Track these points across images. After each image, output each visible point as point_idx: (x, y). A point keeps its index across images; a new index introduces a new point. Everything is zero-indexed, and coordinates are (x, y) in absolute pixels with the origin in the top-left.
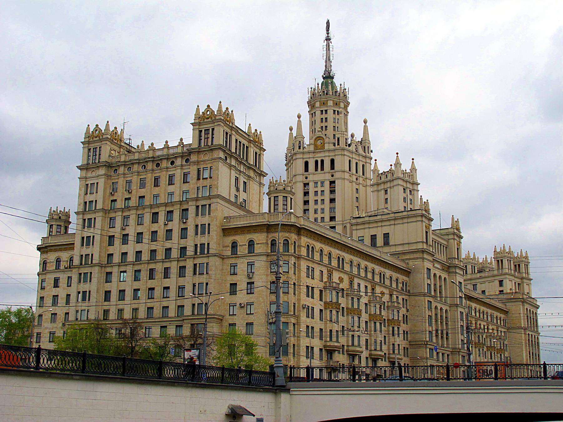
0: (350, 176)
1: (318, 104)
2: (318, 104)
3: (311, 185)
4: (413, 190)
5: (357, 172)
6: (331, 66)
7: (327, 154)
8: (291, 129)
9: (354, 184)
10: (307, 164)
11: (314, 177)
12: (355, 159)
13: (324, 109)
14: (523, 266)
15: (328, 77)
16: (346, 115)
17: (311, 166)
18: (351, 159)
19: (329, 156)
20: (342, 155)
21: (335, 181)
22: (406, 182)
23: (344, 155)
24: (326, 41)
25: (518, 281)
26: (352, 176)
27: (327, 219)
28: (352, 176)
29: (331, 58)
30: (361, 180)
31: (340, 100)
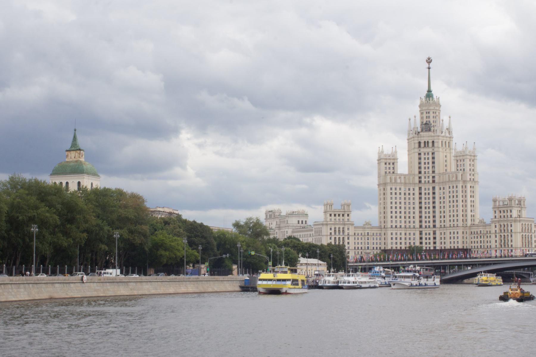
3: (422, 154)
5: (445, 147)
7: (430, 138)
8: (410, 120)
10: (420, 143)
11: (423, 150)
13: (428, 111)
14: (522, 202)
15: (429, 91)
17: (422, 145)
19: (431, 139)
21: (434, 153)
22: (471, 156)
25: (519, 209)
27: (431, 172)
30: (448, 150)
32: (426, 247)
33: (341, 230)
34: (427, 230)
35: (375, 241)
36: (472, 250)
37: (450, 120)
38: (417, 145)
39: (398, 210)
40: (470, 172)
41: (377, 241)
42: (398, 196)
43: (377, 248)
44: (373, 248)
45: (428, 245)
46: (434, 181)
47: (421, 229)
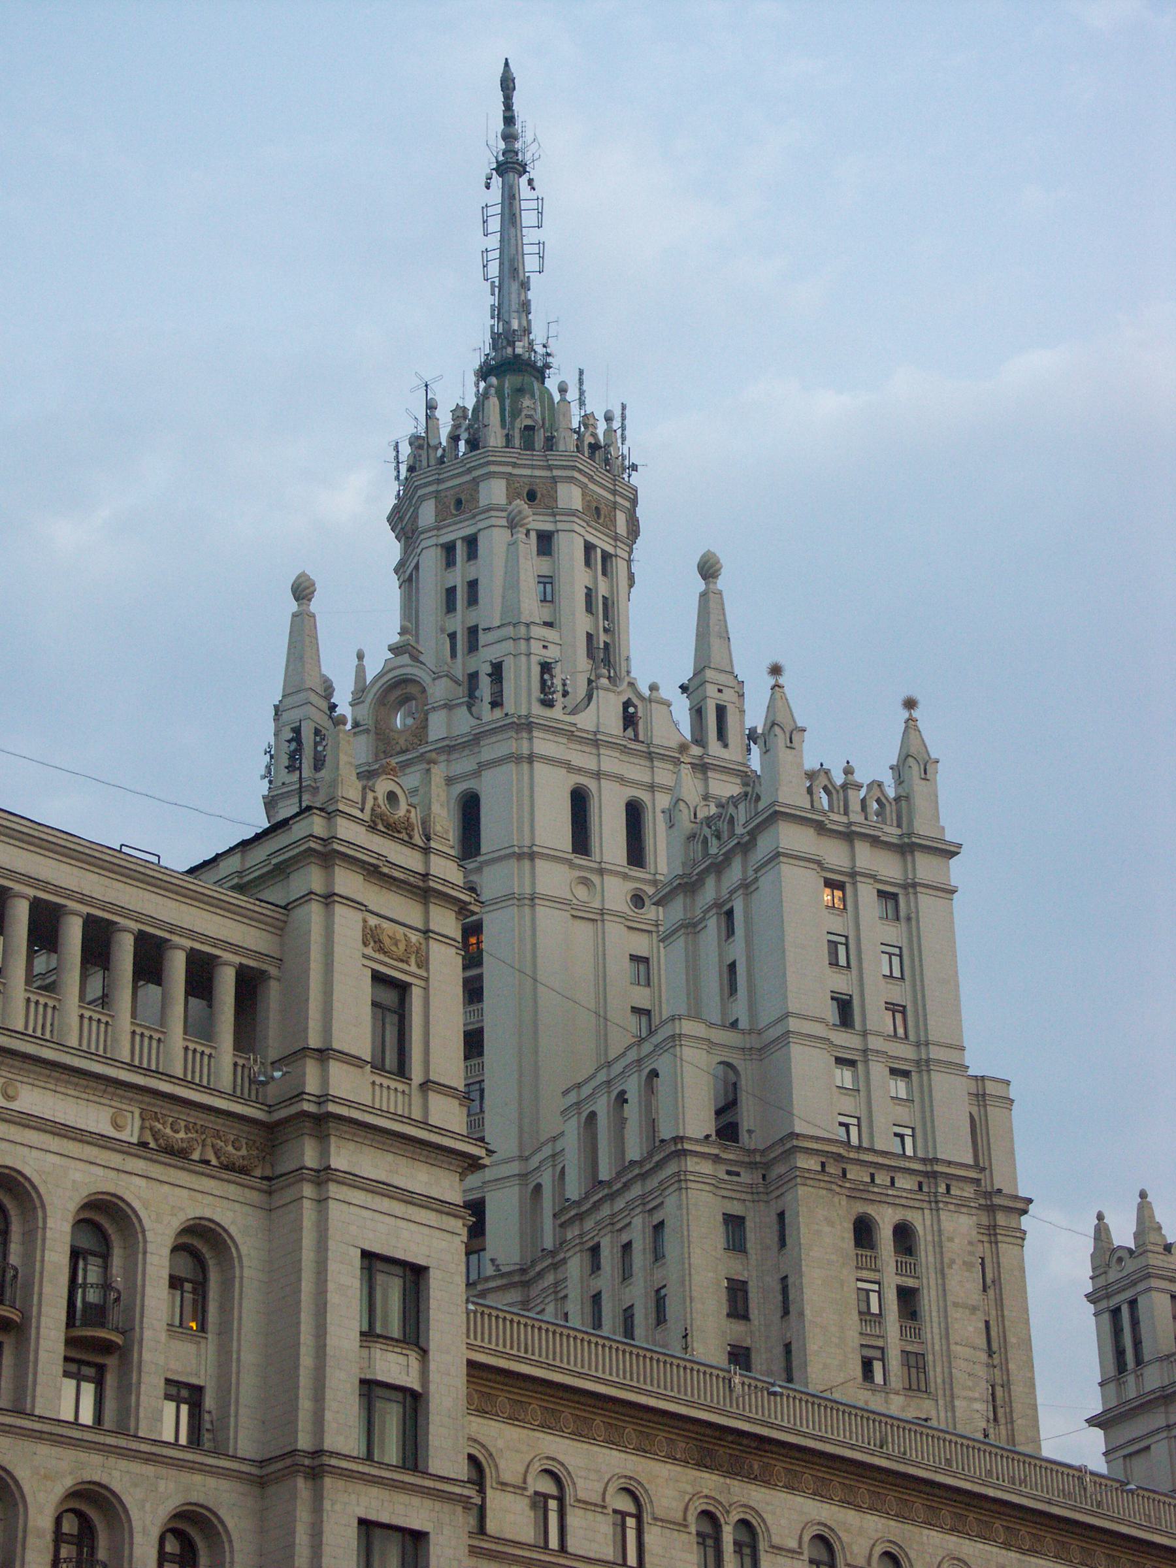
0: (585, 882)
1: (427, 514)
2: (427, 514)
4: (905, 887)
6: (525, 307)
9: (615, 931)
12: (621, 780)
13: (456, 533)
16: (606, 556)
18: (591, 784)
20: (517, 759)
23: (531, 759)
24: (497, 181)
26: (595, 879)
28: (595, 879)
29: (530, 263)
31: (550, 468)
37: (704, 596)
40: (846, 1040)
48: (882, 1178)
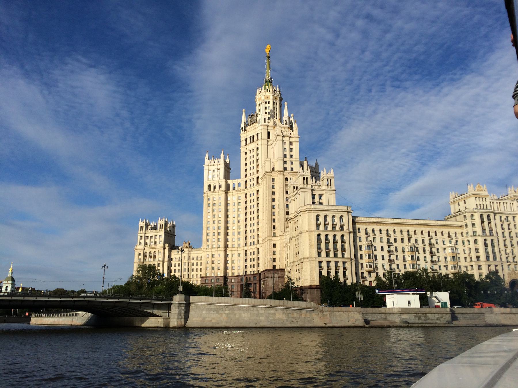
7: (255, 131)
13: (260, 103)
27: (255, 173)
32: (251, 272)
33: (152, 255)
34: (251, 249)
35: (195, 267)
36: (285, 270)
38: (243, 143)
39: (216, 225)
41: (197, 267)
42: (216, 208)
43: (197, 275)
44: (193, 275)
45: (252, 269)
46: (258, 183)
47: (246, 248)
48: (289, 173)
